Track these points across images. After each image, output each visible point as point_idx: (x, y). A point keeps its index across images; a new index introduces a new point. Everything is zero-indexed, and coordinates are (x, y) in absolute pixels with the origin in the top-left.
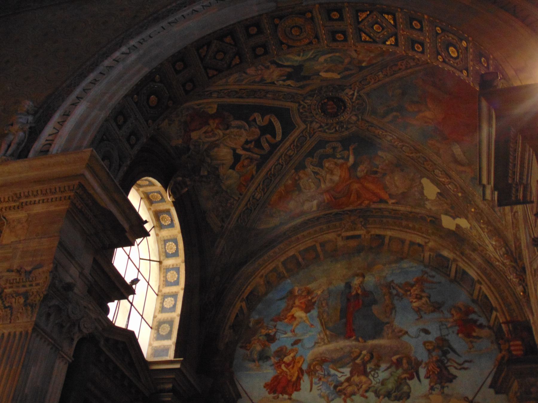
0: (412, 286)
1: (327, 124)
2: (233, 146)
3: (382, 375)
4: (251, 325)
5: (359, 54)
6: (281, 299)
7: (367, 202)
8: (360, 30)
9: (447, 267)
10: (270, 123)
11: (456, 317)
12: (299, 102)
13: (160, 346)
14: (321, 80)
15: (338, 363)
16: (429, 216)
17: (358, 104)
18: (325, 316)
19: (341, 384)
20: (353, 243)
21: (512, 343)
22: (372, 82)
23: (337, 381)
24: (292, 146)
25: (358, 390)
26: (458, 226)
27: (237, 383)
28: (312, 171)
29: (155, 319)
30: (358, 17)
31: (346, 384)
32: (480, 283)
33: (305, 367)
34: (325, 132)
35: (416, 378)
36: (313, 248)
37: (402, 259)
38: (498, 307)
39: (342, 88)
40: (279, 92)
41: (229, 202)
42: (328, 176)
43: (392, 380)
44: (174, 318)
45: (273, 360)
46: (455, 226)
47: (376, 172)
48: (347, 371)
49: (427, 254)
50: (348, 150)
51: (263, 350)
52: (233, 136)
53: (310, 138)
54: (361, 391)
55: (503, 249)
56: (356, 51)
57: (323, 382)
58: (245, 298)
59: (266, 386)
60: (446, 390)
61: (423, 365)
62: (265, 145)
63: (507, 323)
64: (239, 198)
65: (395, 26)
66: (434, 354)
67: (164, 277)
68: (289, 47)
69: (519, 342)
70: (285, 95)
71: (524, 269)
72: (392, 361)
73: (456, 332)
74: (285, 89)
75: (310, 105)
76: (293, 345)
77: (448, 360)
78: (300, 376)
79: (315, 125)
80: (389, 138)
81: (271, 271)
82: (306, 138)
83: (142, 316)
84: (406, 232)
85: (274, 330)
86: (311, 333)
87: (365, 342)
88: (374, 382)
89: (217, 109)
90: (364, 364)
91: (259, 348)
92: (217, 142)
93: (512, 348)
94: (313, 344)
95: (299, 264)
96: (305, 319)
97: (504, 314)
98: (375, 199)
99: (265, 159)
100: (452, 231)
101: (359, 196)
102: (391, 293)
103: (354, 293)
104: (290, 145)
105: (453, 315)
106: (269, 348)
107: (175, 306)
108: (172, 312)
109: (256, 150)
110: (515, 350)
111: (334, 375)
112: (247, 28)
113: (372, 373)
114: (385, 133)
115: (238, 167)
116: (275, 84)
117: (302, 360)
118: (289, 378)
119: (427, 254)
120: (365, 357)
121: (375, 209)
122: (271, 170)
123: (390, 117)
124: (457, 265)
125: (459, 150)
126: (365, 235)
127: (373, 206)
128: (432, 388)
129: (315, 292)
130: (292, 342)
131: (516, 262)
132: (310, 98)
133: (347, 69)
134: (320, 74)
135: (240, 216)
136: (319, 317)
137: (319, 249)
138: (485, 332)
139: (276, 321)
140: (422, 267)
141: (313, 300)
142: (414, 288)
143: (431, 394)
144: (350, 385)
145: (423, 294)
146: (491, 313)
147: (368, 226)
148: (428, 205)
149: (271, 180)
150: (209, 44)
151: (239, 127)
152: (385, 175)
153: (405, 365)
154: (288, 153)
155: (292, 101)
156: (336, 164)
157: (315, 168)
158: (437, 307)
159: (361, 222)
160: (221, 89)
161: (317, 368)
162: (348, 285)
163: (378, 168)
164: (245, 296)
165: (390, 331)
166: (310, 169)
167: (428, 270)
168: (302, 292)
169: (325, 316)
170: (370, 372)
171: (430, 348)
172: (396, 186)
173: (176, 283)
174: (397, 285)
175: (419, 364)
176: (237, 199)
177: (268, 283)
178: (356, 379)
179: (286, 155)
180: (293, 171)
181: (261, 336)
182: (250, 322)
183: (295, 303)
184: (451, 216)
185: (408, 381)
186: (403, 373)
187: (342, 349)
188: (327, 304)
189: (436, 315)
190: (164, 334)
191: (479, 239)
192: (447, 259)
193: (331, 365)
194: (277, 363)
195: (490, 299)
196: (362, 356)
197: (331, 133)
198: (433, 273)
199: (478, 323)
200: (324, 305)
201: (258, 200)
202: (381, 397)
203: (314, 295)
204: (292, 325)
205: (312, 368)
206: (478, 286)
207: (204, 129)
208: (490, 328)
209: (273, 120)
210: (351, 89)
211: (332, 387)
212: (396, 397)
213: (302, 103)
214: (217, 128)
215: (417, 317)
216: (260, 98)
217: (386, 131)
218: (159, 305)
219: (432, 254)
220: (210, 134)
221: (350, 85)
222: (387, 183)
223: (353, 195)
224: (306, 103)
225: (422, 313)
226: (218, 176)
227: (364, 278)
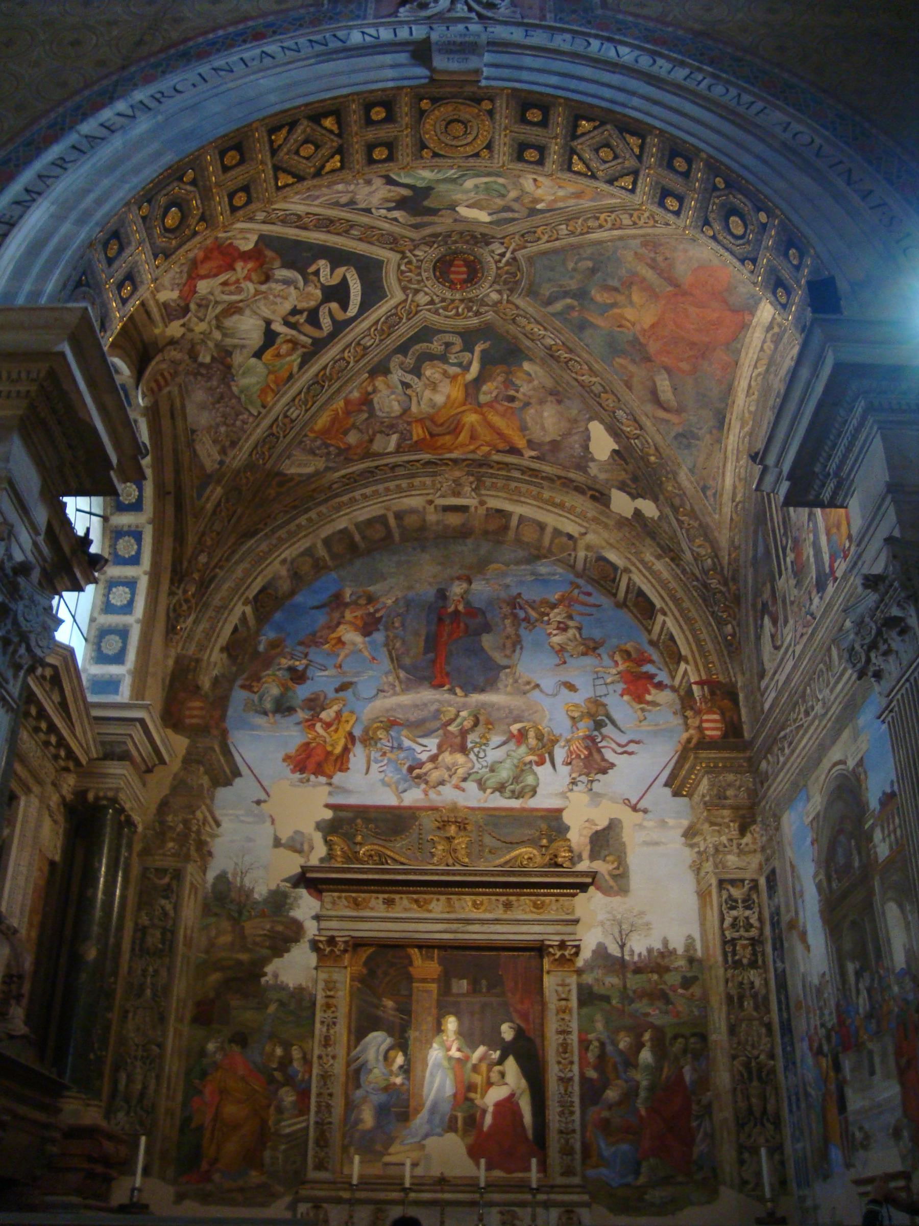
0: (553, 606)
1: (443, 300)
2: (266, 312)
3: (492, 755)
4: (261, 648)
5: (538, 187)
6: (317, 608)
7: (486, 449)
8: (573, 152)
9: (614, 580)
10: (344, 282)
11: (621, 667)
12: (403, 253)
13: (103, 675)
14: (455, 220)
15: (420, 728)
16: (590, 489)
17: (507, 273)
18: (398, 645)
19: (421, 765)
20: (454, 520)
21: (705, 717)
22: (545, 238)
23: (415, 759)
25: (450, 776)
26: (638, 513)
27: (233, 750)
29: (94, 624)
30: (576, 126)
31: (429, 766)
32: (665, 614)
33: (357, 733)
34: (436, 312)
35: (548, 764)
36: (382, 520)
37: (538, 557)
38: (690, 658)
39: (486, 240)
41: (241, 417)
42: (427, 394)
43: (508, 764)
44: (131, 626)
45: (301, 715)
46: (632, 511)
47: (512, 399)
48: (432, 743)
49: (581, 554)
50: (472, 352)
51: (282, 695)
52: (271, 297)
53: (409, 319)
54: (455, 780)
55: (709, 561)
56: (535, 180)
57: (389, 760)
58: (251, 597)
59: (287, 758)
60: (595, 785)
61: (562, 743)
63: (701, 683)
64: (259, 413)
65: (639, 158)
66: (581, 725)
67: (110, 546)
68: (436, 155)
69: (716, 717)
70: (382, 235)
71: (737, 599)
72: (511, 732)
73: (620, 691)
74: (386, 226)
75: (422, 261)
76: (337, 691)
77: (604, 738)
78: (350, 746)
79: (422, 299)
80: (549, 342)
81: (302, 554)
82: (401, 319)
83: (74, 617)
84: (548, 511)
85: (304, 662)
86: (371, 673)
87: (466, 696)
88: (478, 766)
89: (257, 243)
90: (464, 733)
91: (275, 691)
92: (241, 305)
93: (705, 725)
94: (374, 692)
95: (353, 548)
96: (361, 646)
97: (698, 670)
98: (502, 446)
99: (319, 345)
100: (627, 519)
101: (473, 437)
102: (515, 616)
103: (451, 609)
104: (369, 329)
105: (616, 663)
106: (295, 693)
107: (131, 602)
108: (125, 614)
109: (308, 329)
110: (707, 729)
111: (409, 749)
112: (368, 107)
113: (476, 750)
114: (542, 332)
115: (268, 355)
117: (354, 718)
118: (329, 748)
119: (581, 554)
120: (465, 723)
121: (498, 463)
122: (325, 368)
123: (558, 306)
124: (630, 579)
125: (667, 383)
126: (476, 508)
127: (496, 457)
128: (574, 783)
129: (382, 599)
130: (337, 686)
131: (726, 584)
132: (427, 249)
133: (508, 209)
134: (458, 209)
135: (256, 447)
136: (386, 645)
137: (392, 522)
138: (665, 697)
139: (309, 646)
140: (571, 577)
141: (378, 615)
142: (556, 611)
143: (571, 790)
144: (436, 768)
145: (571, 623)
146: (678, 663)
147: (483, 492)
148: (593, 469)
150: (292, 125)
151: (287, 282)
152: (527, 404)
153: (532, 741)
155: (391, 249)
156: (445, 373)
158: (591, 648)
159: (471, 483)
161: (381, 734)
162: (442, 595)
163: (517, 391)
164: (251, 594)
165: (511, 681)
166: (397, 375)
167: (581, 582)
168: (359, 597)
169: (398, 645)
170: (472, 748)
171: (576, 714)
172: (543, 428)
173: (135, 560)
174: (527, 602)
175: (554, 742)
177: (296, 576)
178: (447, 758)
179: (359, 344)
181: (279, 669)
182: (260, 642)
183: (343, 617)
184: (629, 494)
185: (534, 767)
186: (528, 754)
187: (425, 705)
188: (403, 625)
189: (589, 661)
190: (110, 653)
191: (671, 539)
192: (615, 567)
193: (405, 732)
194: (307, 721)
195: (679, 643)
196: (459, 720)
197: (446, 317)
198: (590, 589)
199: (656, 680)
200: (397, 625)
201: (292, 421)
202: (489, 791)
203: (379, 606)
204: (338, 655)
205: (371, 733)
206: (660, 618)
207: (222, 278)
208: (674, 689)
209: (348, 276)
210: (502, 244)
211: (405, 769)
212: (513, 792)
213: (409, 254)
214: (248, 278)
215: (557, 661)
216: (338, 234)
217: (545, 329)
218: (100, 598)
219: (590, 554)
220: (233, 288)
221: (504, 238)
222: (528, 419)
223: (462, 435)
224: (415, 256)
225: (566, 655)
226: (229, 367)
227: (470, 582)
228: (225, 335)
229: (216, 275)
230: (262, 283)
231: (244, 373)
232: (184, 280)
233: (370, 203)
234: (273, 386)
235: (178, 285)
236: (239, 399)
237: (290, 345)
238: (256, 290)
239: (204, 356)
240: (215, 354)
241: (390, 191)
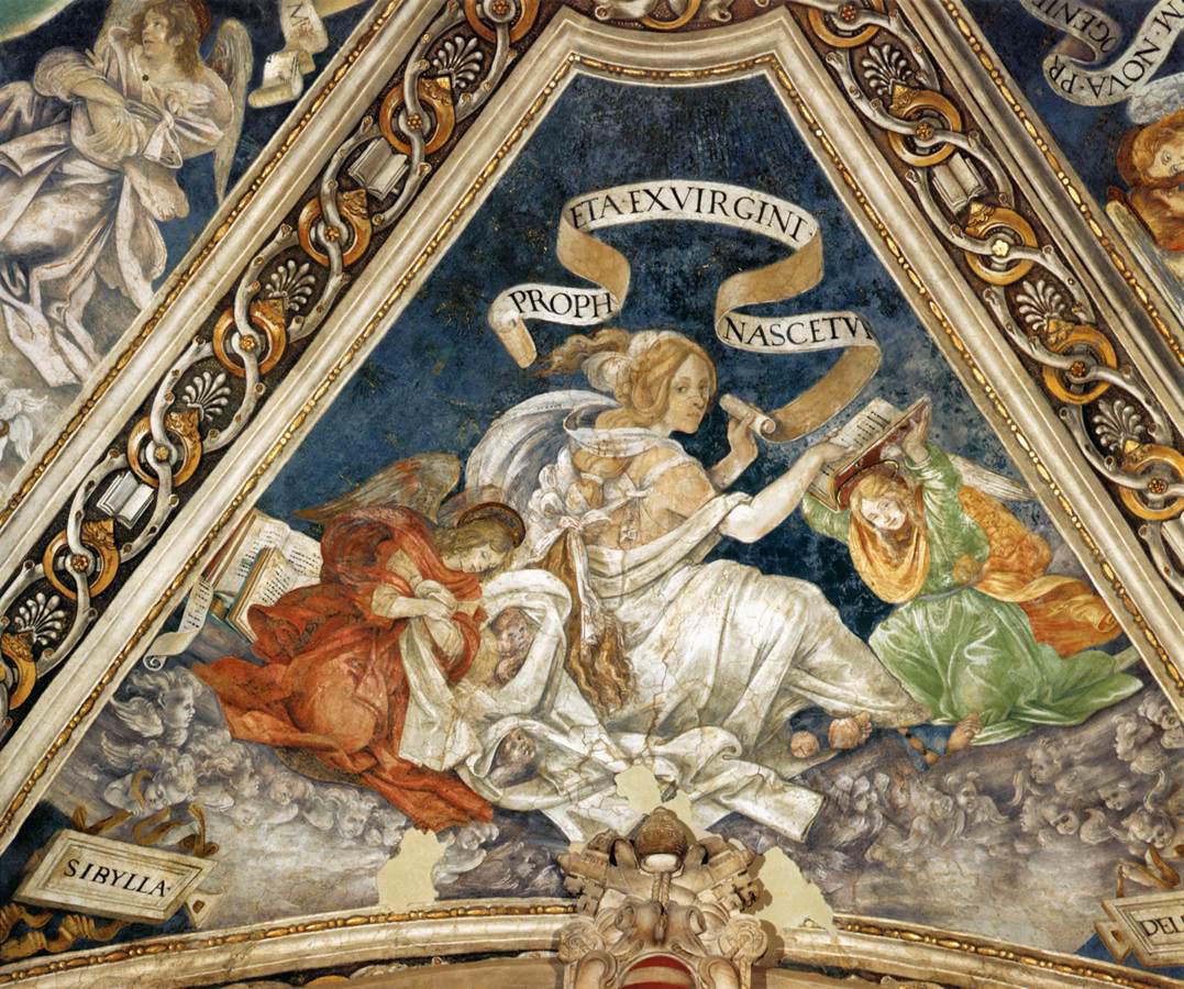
24: (908, 157)
28: (1163, 72)
40: (378, 102)
41: (1120, 749)
52: (595, 515)
62: (797, 334)
70: (429, 75)
92: (588, 632)
104: (899, 167)
115: (875, 572)
116: (290, 105)
149: (1114, 392)
151: (546, 447)
154: (955, 207)
155: (521, 48)
157: (1139, 43)
160: (106, 439)
176: (1139, 684)
179: (960, 220)
180: (1111, 207)
214: (465, 585)
216: (381, 236)
220: (489, 642)
226: (878, 734)
228: (710, 717)
229: (401, 693)
230: (516, 534)
231: (934, 690)
232: (360, 806)
233: (209, 111)
234: (1040, 588)
235: (374, 824)
236: (1039, 730)
237: (867, 484)
238: (545, 564)
239: (787, 811)
240: (795, 770)
241: (137, 36)
